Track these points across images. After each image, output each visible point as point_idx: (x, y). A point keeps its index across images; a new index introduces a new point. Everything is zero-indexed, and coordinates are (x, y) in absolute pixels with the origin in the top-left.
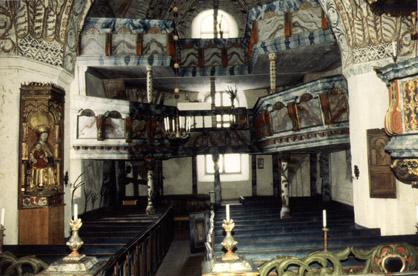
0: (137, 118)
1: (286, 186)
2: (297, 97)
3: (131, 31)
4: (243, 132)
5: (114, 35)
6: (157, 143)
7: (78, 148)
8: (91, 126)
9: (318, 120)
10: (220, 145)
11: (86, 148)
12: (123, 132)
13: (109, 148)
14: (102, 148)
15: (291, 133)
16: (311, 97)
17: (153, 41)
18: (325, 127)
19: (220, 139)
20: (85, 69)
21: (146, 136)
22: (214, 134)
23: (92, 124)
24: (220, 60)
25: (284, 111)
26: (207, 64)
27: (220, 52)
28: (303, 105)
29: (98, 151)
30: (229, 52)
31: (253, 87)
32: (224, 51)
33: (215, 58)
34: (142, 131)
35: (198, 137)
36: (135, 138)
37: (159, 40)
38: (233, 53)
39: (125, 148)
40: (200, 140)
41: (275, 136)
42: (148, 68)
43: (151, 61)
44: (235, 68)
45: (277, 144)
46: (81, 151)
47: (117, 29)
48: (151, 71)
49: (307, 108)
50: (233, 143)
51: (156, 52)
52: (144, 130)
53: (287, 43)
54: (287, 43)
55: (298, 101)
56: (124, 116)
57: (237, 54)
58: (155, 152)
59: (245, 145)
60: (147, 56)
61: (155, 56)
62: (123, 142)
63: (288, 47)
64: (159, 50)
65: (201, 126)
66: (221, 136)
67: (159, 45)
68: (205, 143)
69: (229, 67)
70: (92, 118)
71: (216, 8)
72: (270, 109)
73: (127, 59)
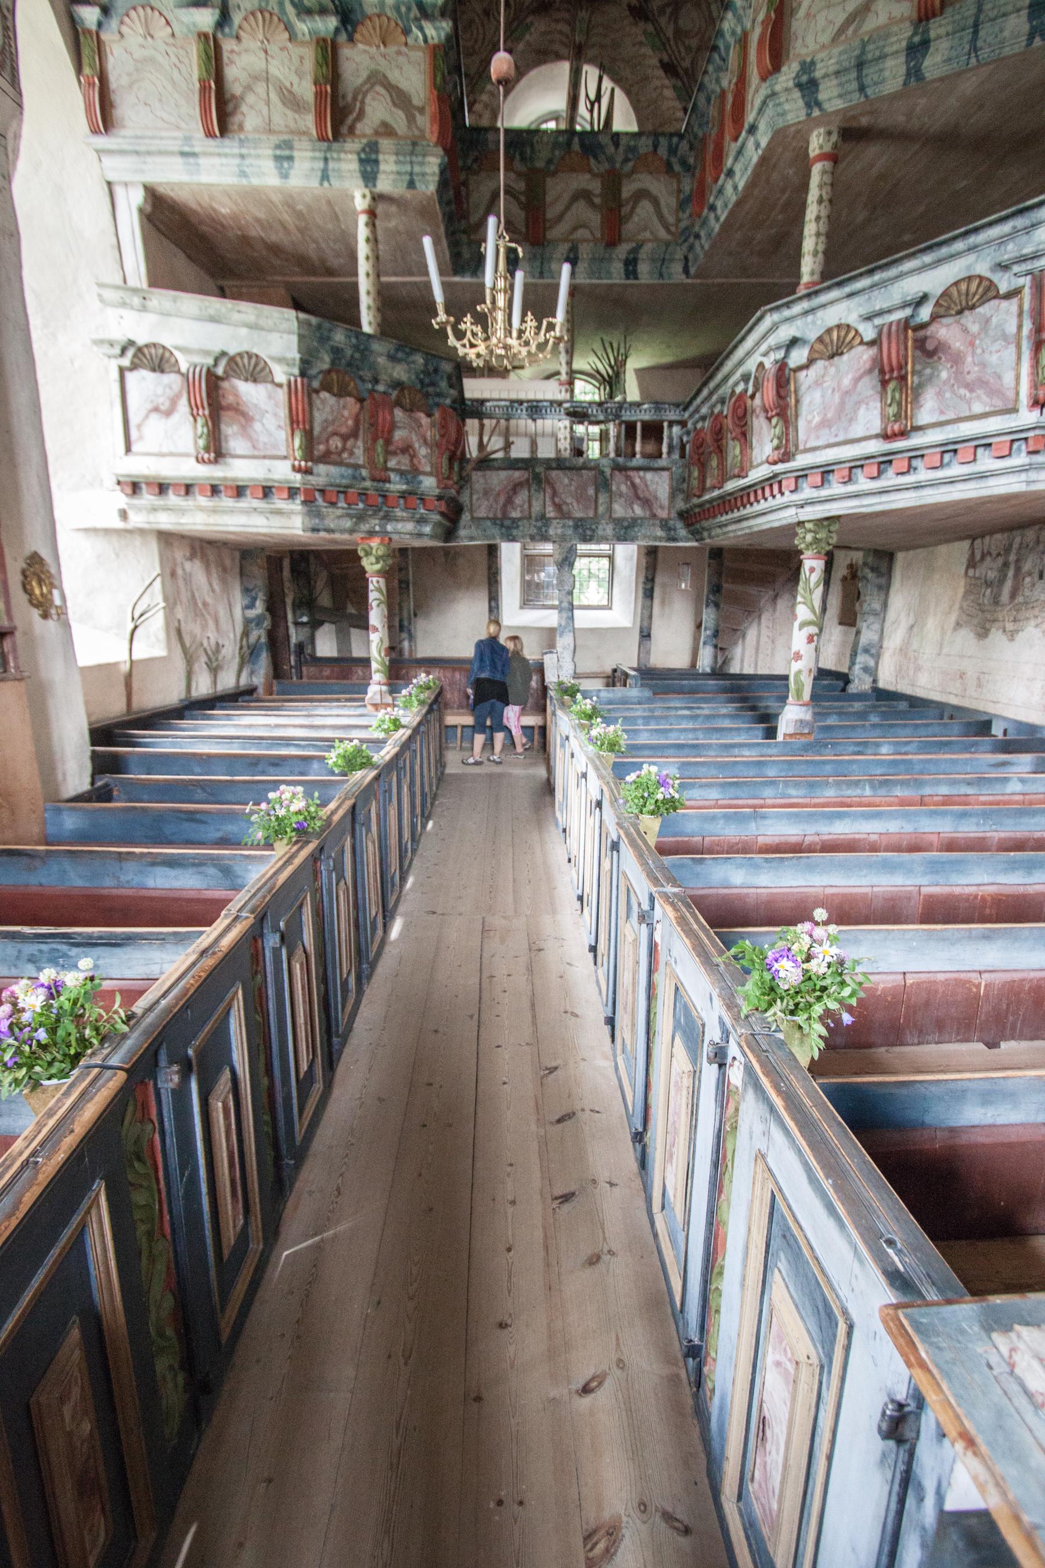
0: (326, 387)
1: (810, 639)
2: (924, 298)
3: (289, 28)
4: (649, 476)
5: (228, 45)
6: (396, 485)
7: (135, 488)
8: (168, 413)
9: (994, 392)
10: (579, 515)
11: (162, 488)
12: (282, 435)
13: (239, 491)
14: (215, 490)
15: (875, 447)
16: (989, 292)
17: (377, 79)
18: (1028, 417)
19: (581, 496)
20: (137, 197)
21: (359, 455)
22: (562, 479)
23: (174, 402)
24: (595, 219)
25: (861, 357)
26: (554, 233)
27: (595, 186)
28: (945, 332)
29: (202, 501)
30: (627, 190)
31: (667, 359)
32: (613, 181)
33: (581, 210)
34: (345, 438)
35: (516, 488)
36: (325, 458)
37: (395, 76)
38: (643, 194)
39: (292, 492)
40: (518, 500)
41: (801, 461)
42: (360, 202)
43: (369, 174)
44: (643, 254)
45: (807, 492)
46: (147, 498)
47: (237, 18)
48: (372, 213)
49: (957, 344)
50: (619, 510)
51: (386, 130)
52: (354, 434)
53: (917, 50)
54: (917, 50)
55: (925, 313)
56: (280, 374)
57: (656, 202)
58: (387, 518)
59: (654, 516)
60: (354, 145)
61: (385, 143)
62: (283, 472)
63: (914, 73)
64: (399, 120)
65: (526, 454)
66: (583, 488)
67: (400, 98)
68: (536, 507)
69: (623, 250)
70: (171, 381)
71: (578, 55)
72: (798, 356)
73: (284, 159)
